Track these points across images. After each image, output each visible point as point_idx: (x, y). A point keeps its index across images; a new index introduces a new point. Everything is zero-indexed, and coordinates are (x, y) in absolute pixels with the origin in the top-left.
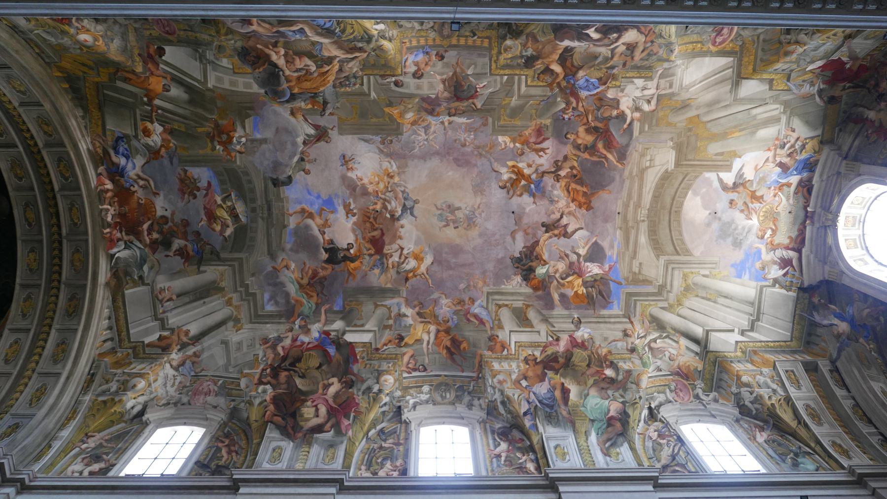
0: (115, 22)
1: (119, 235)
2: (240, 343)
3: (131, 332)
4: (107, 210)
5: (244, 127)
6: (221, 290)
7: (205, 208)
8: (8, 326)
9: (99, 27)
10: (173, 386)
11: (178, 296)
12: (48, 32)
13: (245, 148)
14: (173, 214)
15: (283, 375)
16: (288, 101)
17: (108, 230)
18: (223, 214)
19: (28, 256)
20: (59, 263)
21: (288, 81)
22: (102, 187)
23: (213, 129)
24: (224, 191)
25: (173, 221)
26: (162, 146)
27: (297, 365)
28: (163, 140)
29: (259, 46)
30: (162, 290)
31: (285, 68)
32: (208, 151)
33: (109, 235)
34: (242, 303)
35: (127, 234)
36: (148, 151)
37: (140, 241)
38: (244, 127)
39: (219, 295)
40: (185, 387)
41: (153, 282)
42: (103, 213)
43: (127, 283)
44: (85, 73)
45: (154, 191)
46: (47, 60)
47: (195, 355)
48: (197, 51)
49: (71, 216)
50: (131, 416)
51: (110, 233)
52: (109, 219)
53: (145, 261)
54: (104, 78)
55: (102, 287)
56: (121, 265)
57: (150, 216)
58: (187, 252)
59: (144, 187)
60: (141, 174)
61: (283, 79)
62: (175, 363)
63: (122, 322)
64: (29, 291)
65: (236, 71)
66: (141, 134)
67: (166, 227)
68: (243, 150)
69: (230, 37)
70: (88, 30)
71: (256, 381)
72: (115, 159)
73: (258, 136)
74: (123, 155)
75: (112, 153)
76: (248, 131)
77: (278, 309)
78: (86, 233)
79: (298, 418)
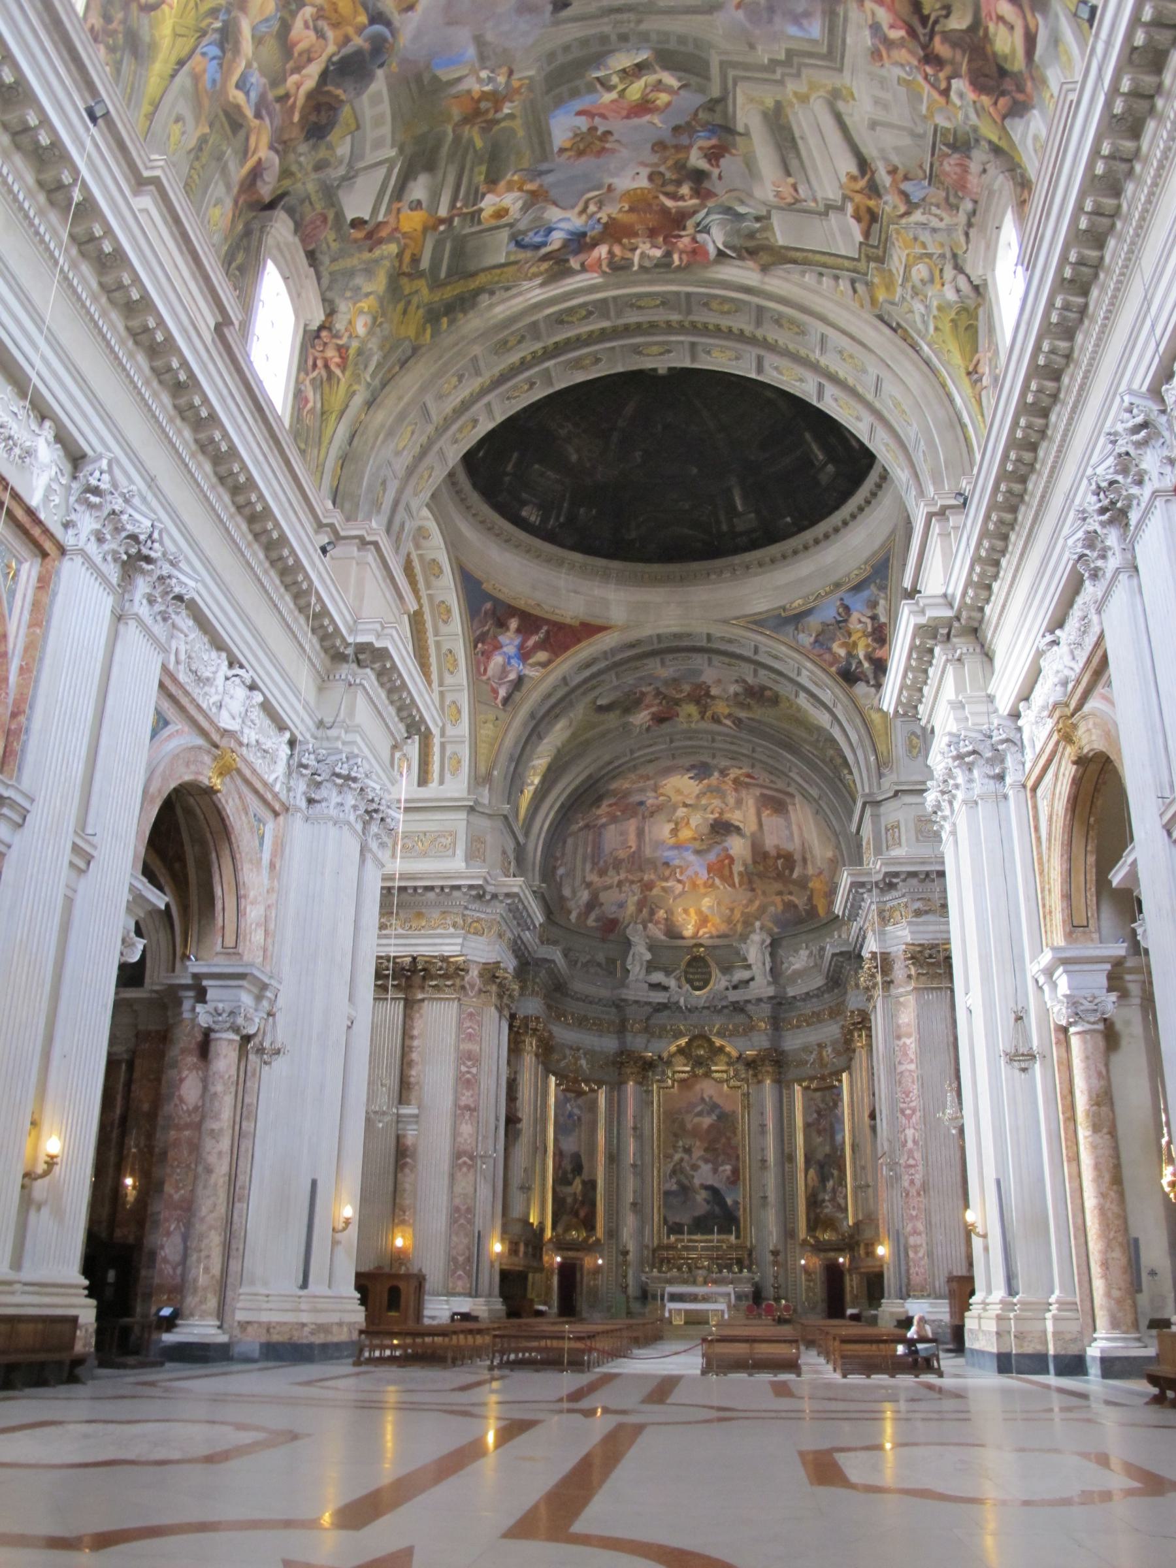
0: (330, 288)
1: (686, 240)
2: (877, 102)
3: (843, 253)
4: (643, 255)
5: (459, 80)
6: (779, 107)
7: (628, 117)
8: (815, 403)
9: (343, 307)
10: (941, 220)
11: (788, 174)
12: (366, 367)
13: (500, 67)
14: (645, 165)
15: (940, 47)
16: (388, 23)
17: (676, 257)
18: (635, 91)
21: (347, 40)
22: (604, 264)
23: (473, 125)
24: (591, 89)
25: (657, 165)
26: (520, 189)
27: (926, 12)
28: (510, 188)
29: (296, 118)
30: (778, 194)
31: (324, 57)
32: (517, 124)
33: (684, 257)
34: (804, 76)
35: (684, 229)
36: (533, 204)
37: (695, 212)
38: (459, 80)
39: (789, 111)
40: (947, 199)
41: (765, 203)
42: (647, 264)
44: (418, 307)
45: (604, 190)
46: (409, 352)
47: (893, 171)
48: (338, 186)
50: (972, 294)
51: (681, 252)
52: (658, 253)
54: (422, 285)
55: (767, 279)
56: (737, 242)
58: (713, 147)
59: (601, 205)
61: (346, 51)
62: (902, 209)
65: (353, 127)
66: (504, 220)
67: (668, 175)
68: (504, 70)
69: (294, 168)
70: (350, 322)
71: (941, 100)
72: (556, 245)
73: (471, 52)
75: (544, 251)
76: (466, 72)
77: (818, 15)
78: (677, 294)
79: (1007, 66)
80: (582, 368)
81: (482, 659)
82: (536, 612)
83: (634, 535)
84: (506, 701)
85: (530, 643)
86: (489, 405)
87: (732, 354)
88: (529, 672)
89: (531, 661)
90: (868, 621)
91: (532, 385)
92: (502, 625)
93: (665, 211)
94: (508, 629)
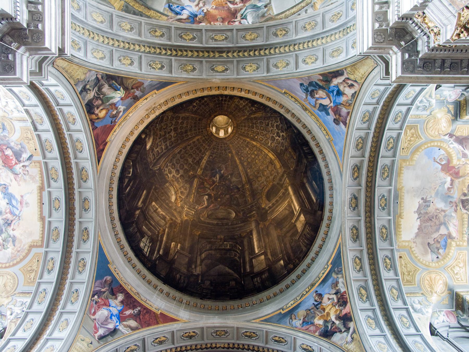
1: (237, 23)
19: (248, 71)
20: (253, 51)
35: (236, 18)
37: (241, 9)
43: (270, 14)
49: (220, 41)
53: (255, 5)
57: (224, 3)
60: (196, 3)
63: (295, 10)
64: (271, 67)
74: (182, 10)
75: (179, 17)
80: (186, 71)
81: (95, 305)
82: (135, 297)
83: (198, 271)
84: (101, 338)
85: (128, 312)
86: (140, 57)
87: (254, 66)
88: (121, 328)
89: (125, 323)
90: (334, 296)
91: (163, 67)
92: (113, 294)
93: (229, 9)
94: (116, 298)
